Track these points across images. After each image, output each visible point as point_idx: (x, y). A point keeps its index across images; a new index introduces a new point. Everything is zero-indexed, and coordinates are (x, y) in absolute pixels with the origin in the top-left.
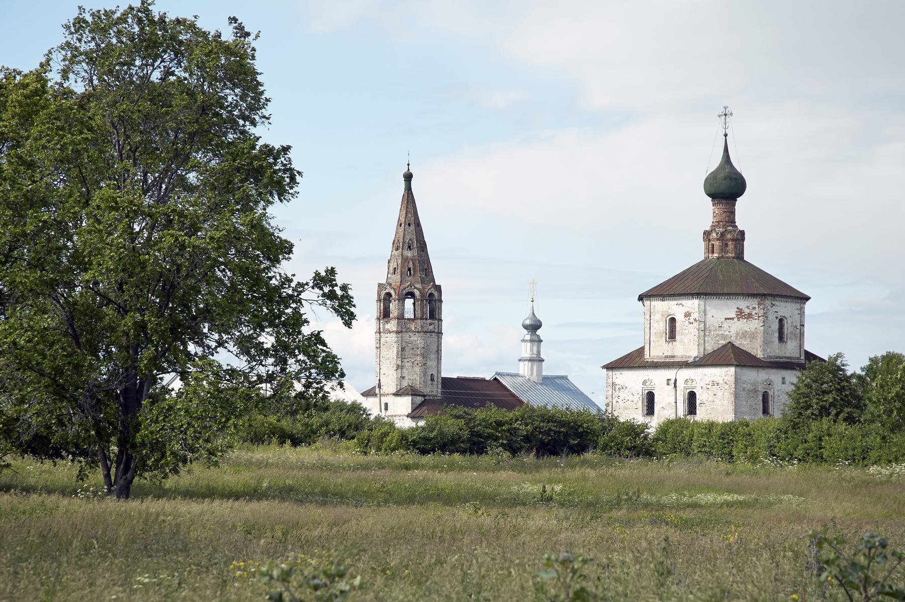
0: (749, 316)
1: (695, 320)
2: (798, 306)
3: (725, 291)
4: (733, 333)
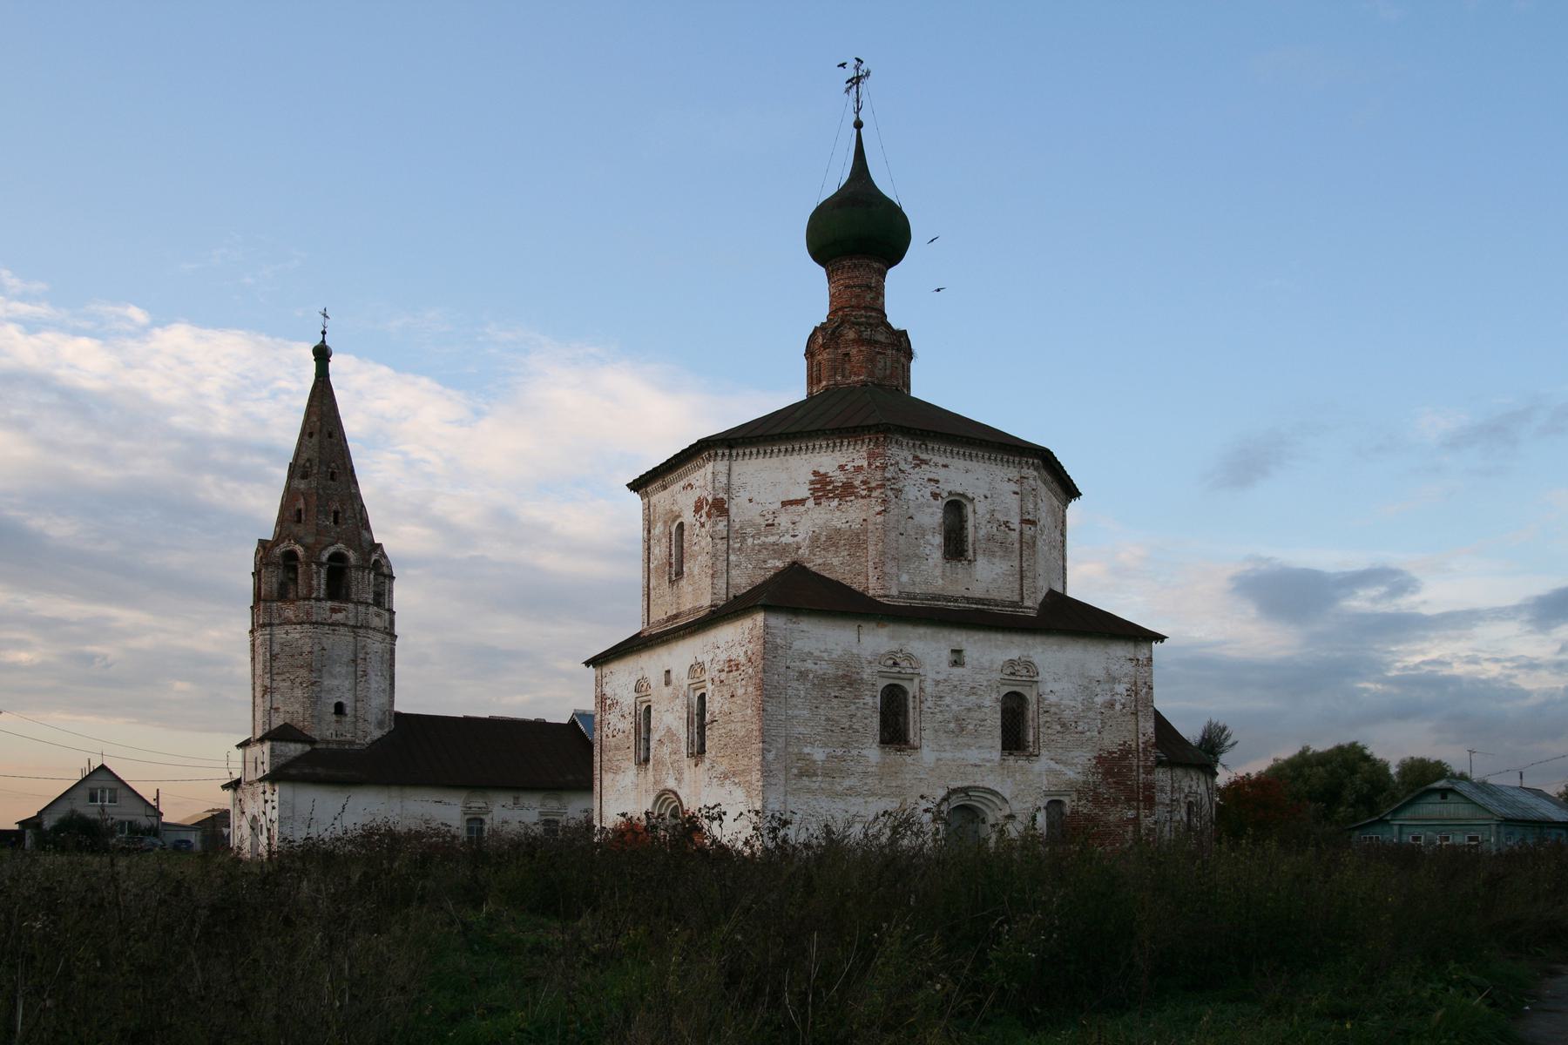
0: (847, 490)
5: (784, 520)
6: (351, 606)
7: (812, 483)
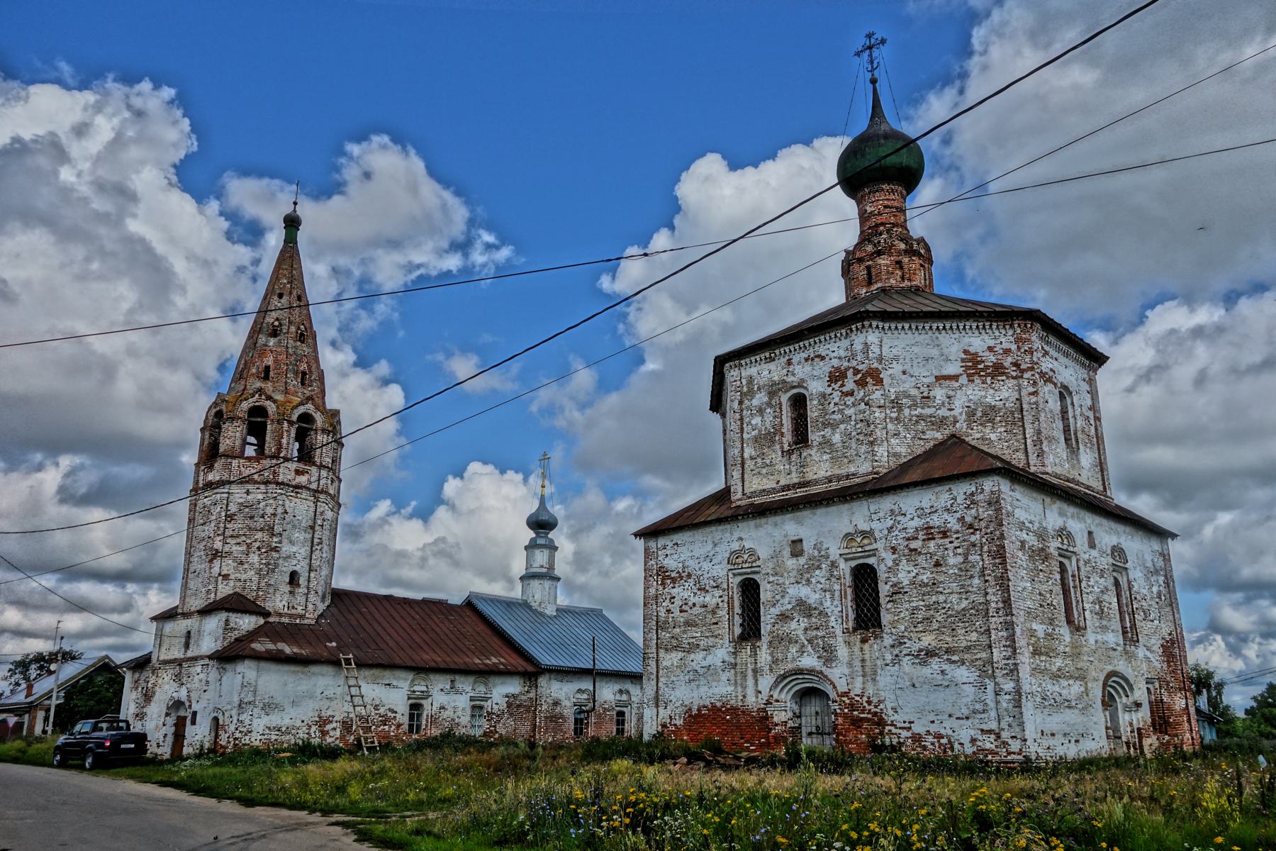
0: (998, 370)
5: (939, 394)
6: (314, 469)
7: (963, 360)
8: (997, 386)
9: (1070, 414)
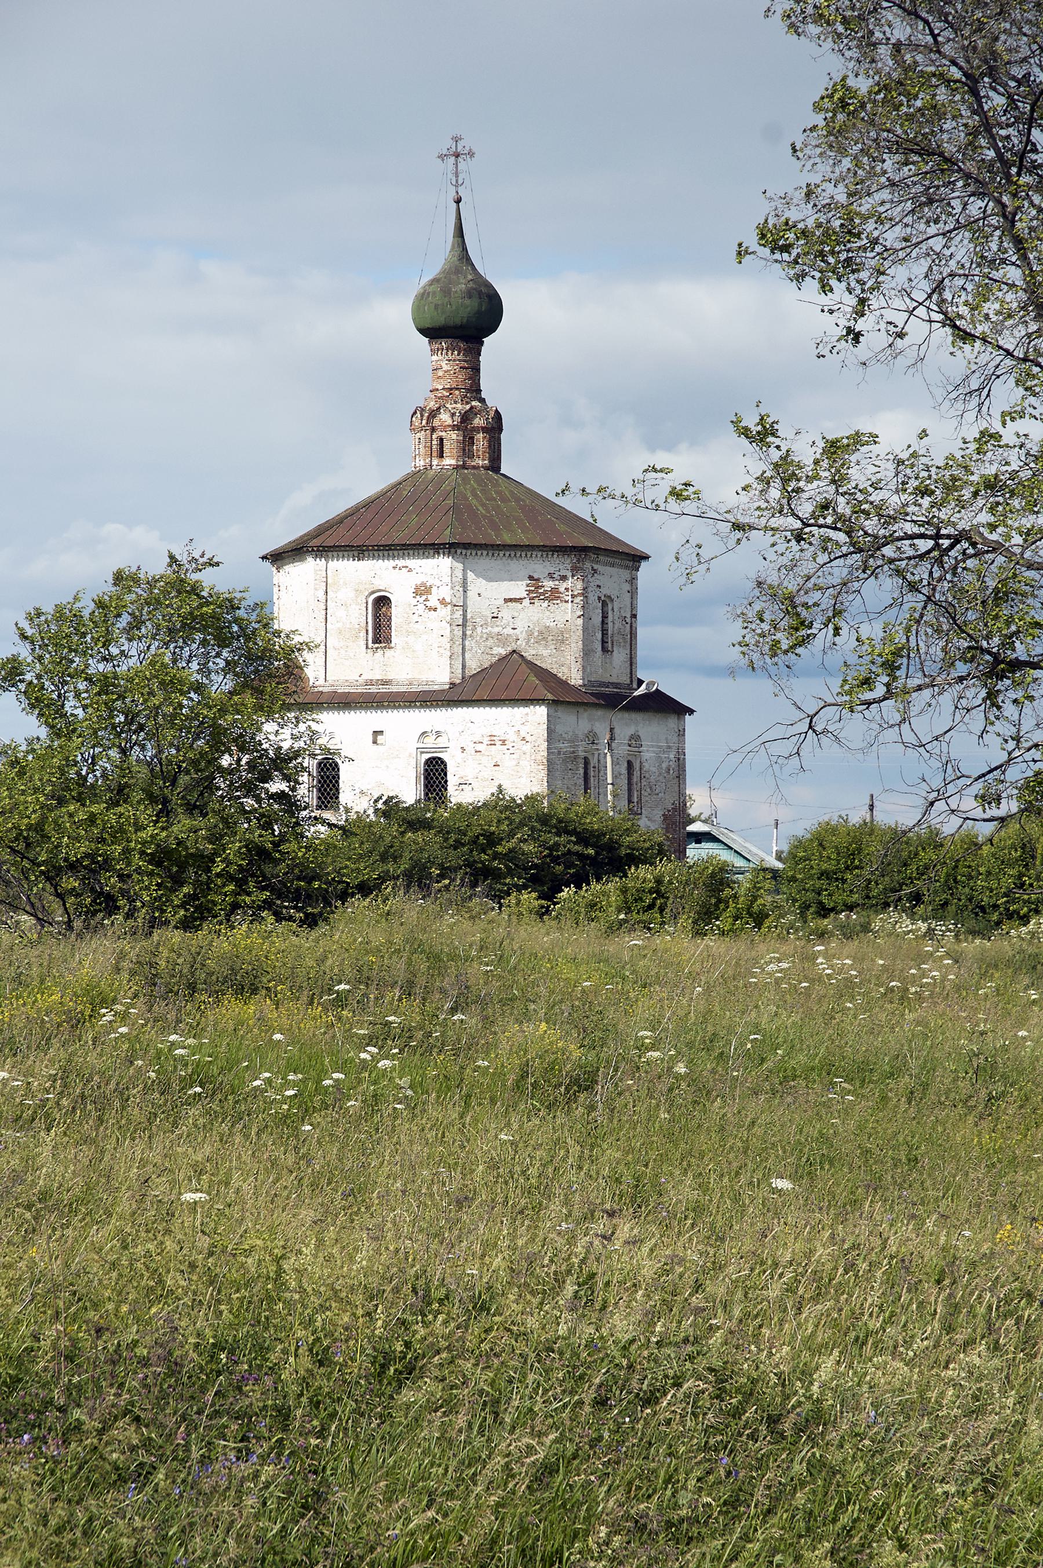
0: (554, 595)
1: (443, 602)
2: (626, 574)
3: (507, 538)
4: (521, 632)
5: (506, 613)
8: (552, 608)
9: (610, 619)
